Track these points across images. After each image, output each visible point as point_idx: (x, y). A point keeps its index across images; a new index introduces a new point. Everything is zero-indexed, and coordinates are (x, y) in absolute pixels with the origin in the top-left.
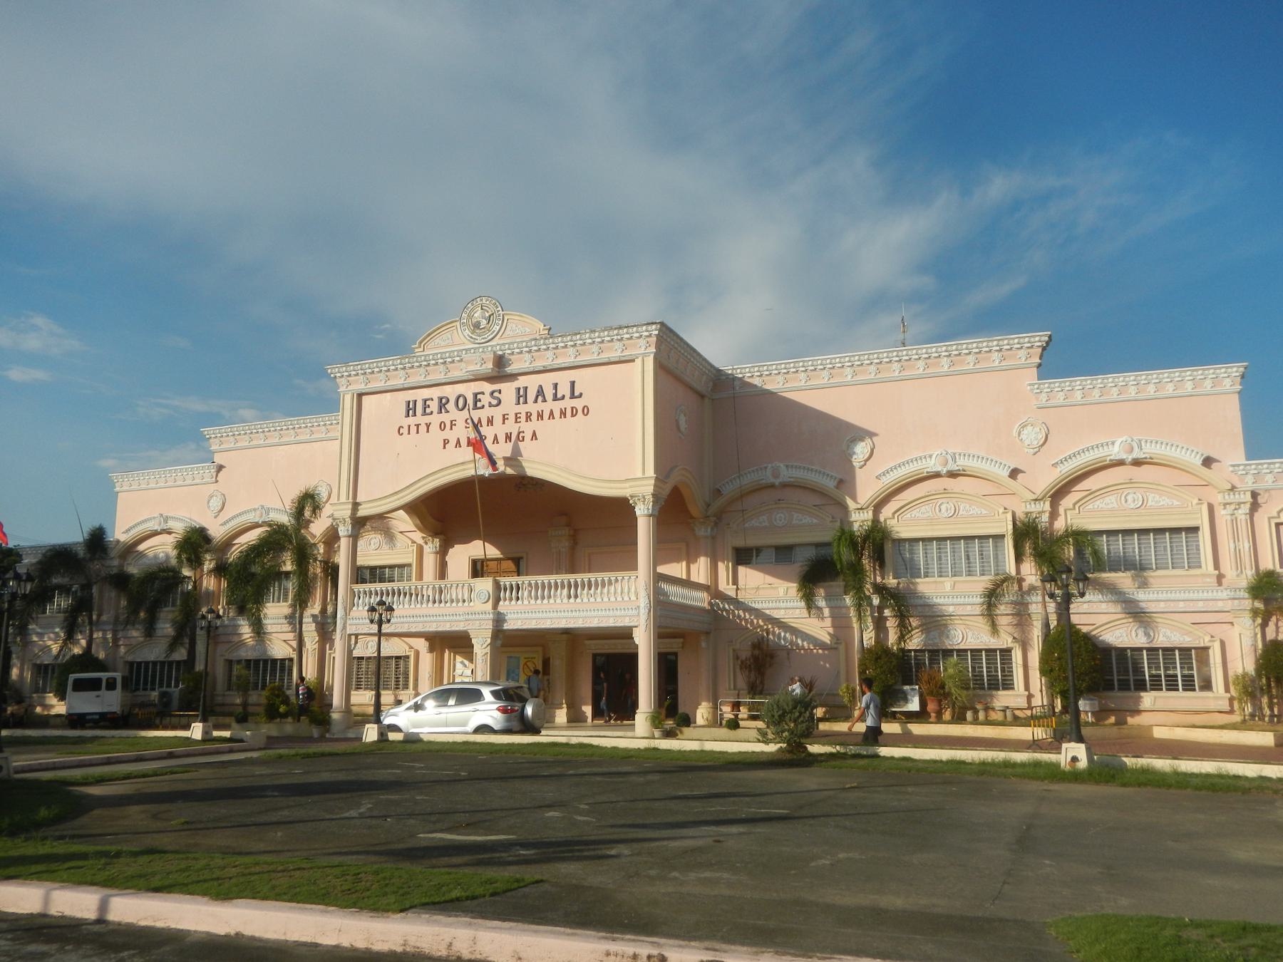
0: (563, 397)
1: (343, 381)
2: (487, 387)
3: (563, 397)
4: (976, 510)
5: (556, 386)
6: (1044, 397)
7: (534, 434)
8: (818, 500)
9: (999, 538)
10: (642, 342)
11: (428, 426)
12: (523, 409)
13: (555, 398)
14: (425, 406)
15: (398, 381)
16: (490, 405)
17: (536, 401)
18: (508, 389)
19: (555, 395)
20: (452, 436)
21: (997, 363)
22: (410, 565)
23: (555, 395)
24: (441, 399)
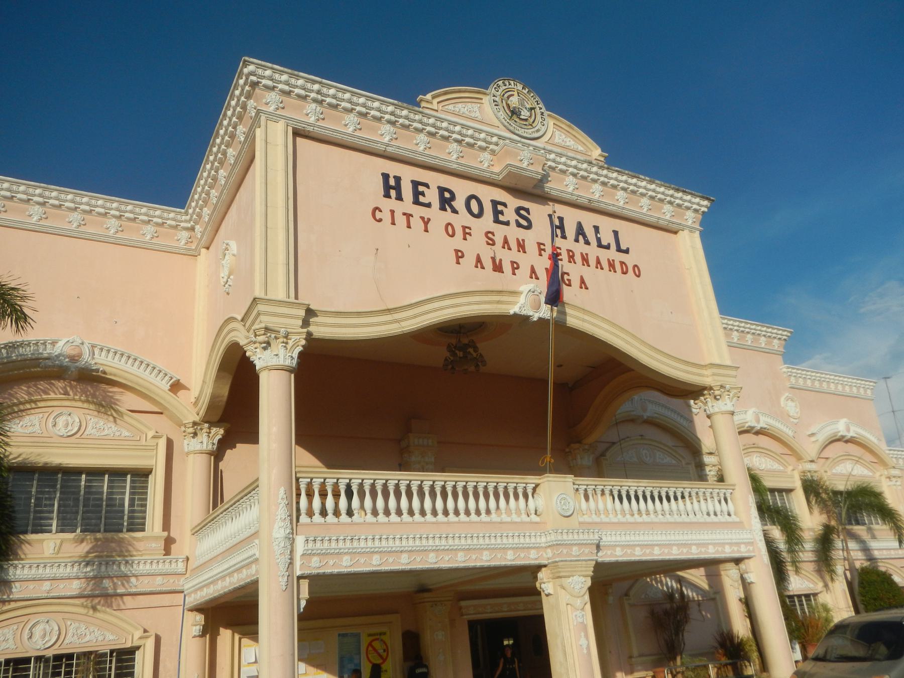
0: (608, 247)
1: (273, 96)
2: (513, 202)
3: (608, 247)
4: (776, 466)
5: (597, 229)
6: (793, 380)
7: (582, 281)
8: (669, 441)
9: (789, 491)
10: (690, 214)
11: (426, 222)
13: (600, 245)
14: (417, 194)
15: (383, 135)
16: (519, 225)
17: (577, 240)
18: (539, 212)
19: (599, 240)
21: (763, 345)
22: (142, 475)
23: (599, 240)
24: (442, 190)
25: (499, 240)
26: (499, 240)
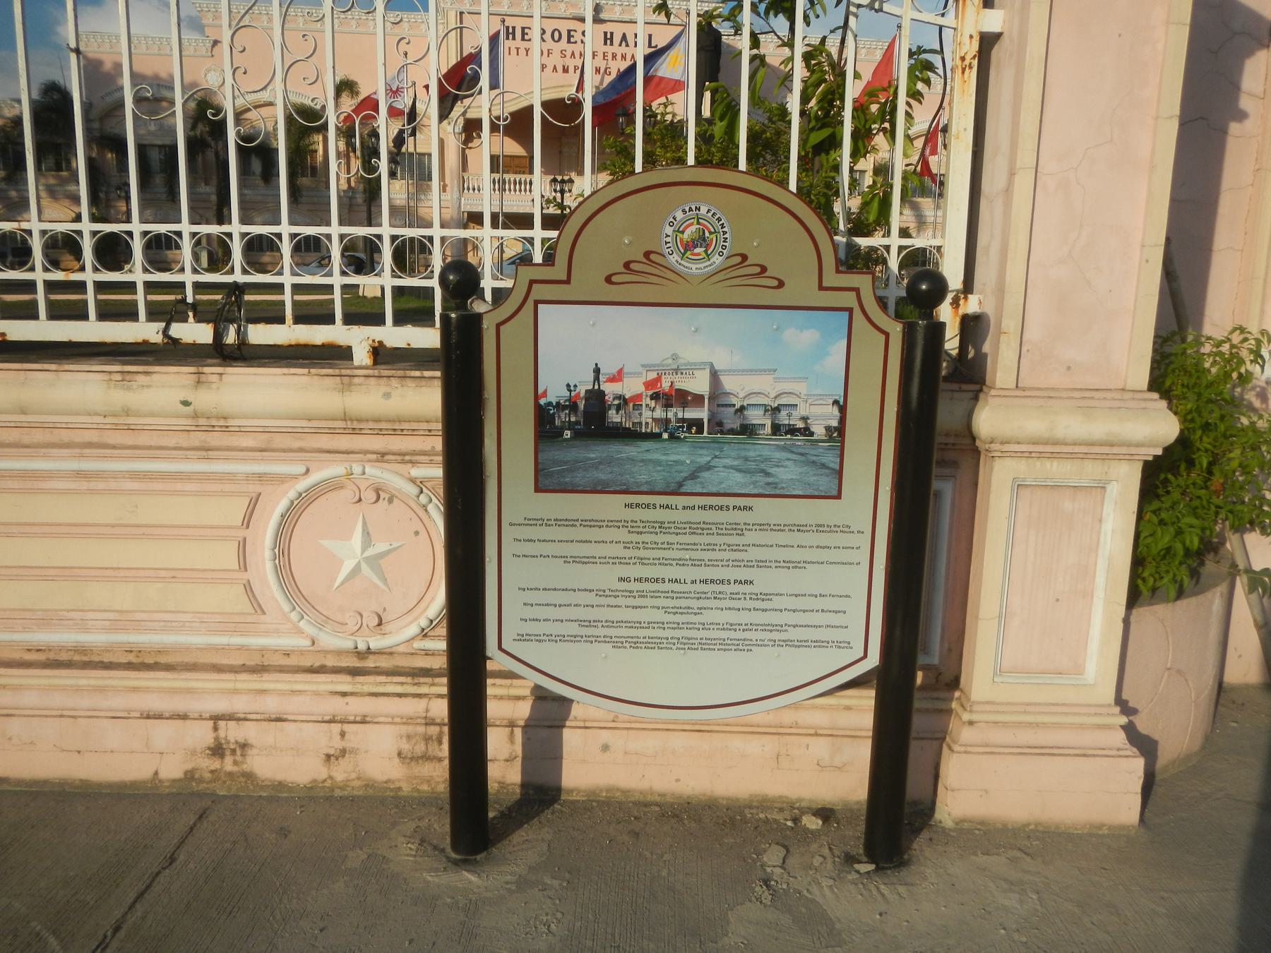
12: (609, 49)
20: (550, 62)
25: (568, 54)
26: (568, 54)
